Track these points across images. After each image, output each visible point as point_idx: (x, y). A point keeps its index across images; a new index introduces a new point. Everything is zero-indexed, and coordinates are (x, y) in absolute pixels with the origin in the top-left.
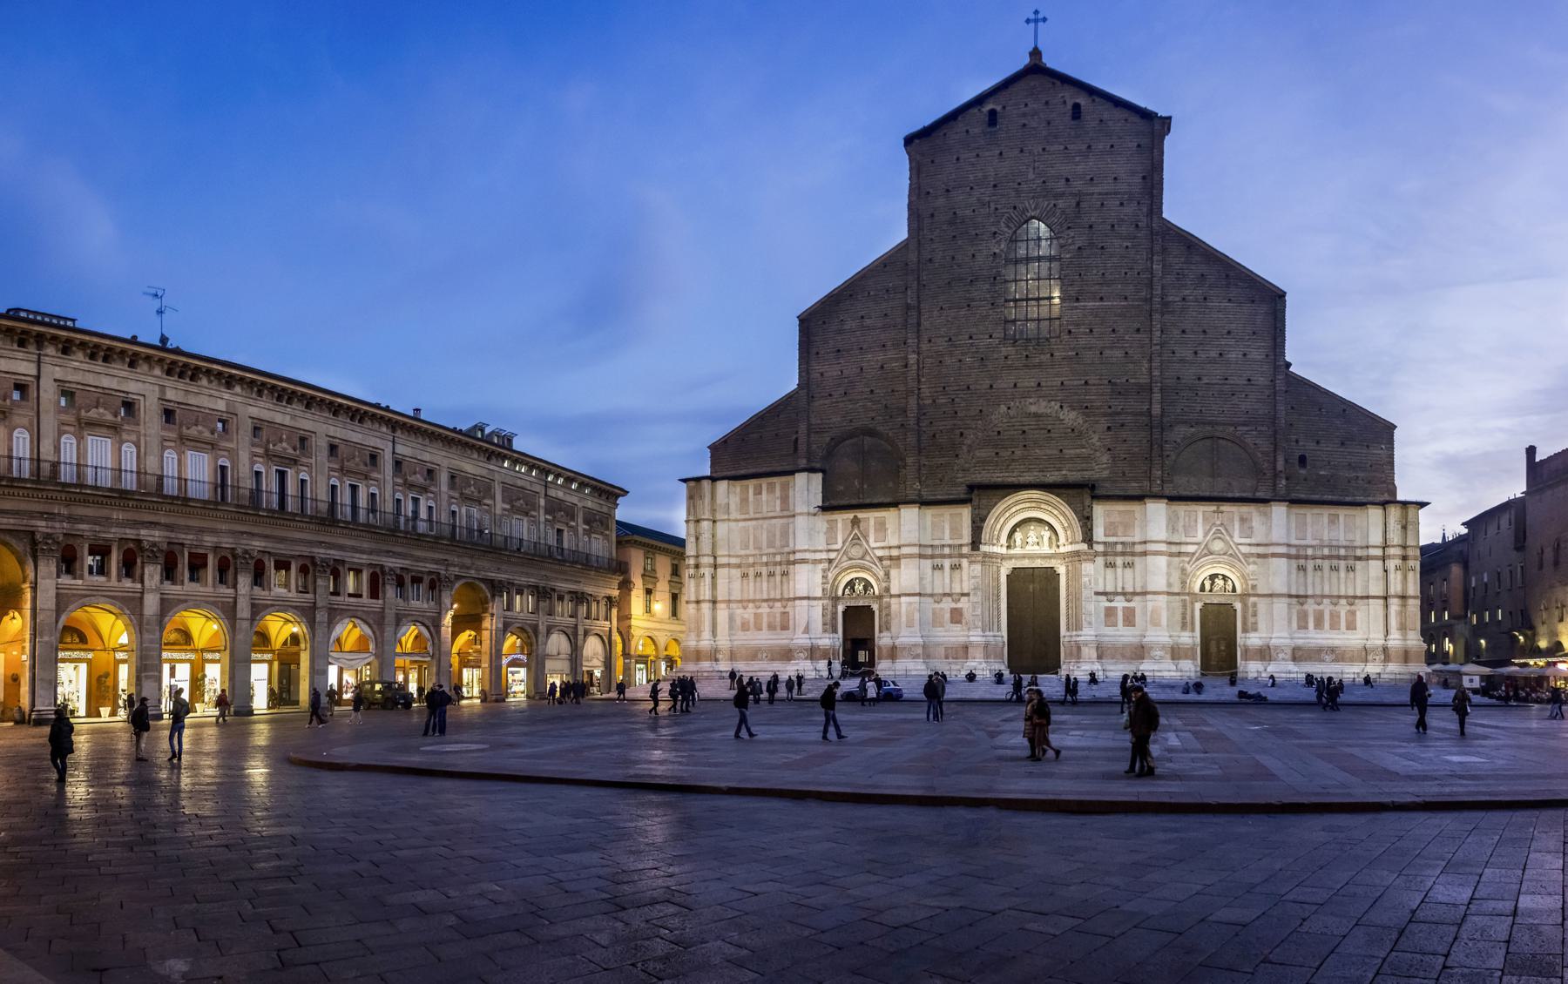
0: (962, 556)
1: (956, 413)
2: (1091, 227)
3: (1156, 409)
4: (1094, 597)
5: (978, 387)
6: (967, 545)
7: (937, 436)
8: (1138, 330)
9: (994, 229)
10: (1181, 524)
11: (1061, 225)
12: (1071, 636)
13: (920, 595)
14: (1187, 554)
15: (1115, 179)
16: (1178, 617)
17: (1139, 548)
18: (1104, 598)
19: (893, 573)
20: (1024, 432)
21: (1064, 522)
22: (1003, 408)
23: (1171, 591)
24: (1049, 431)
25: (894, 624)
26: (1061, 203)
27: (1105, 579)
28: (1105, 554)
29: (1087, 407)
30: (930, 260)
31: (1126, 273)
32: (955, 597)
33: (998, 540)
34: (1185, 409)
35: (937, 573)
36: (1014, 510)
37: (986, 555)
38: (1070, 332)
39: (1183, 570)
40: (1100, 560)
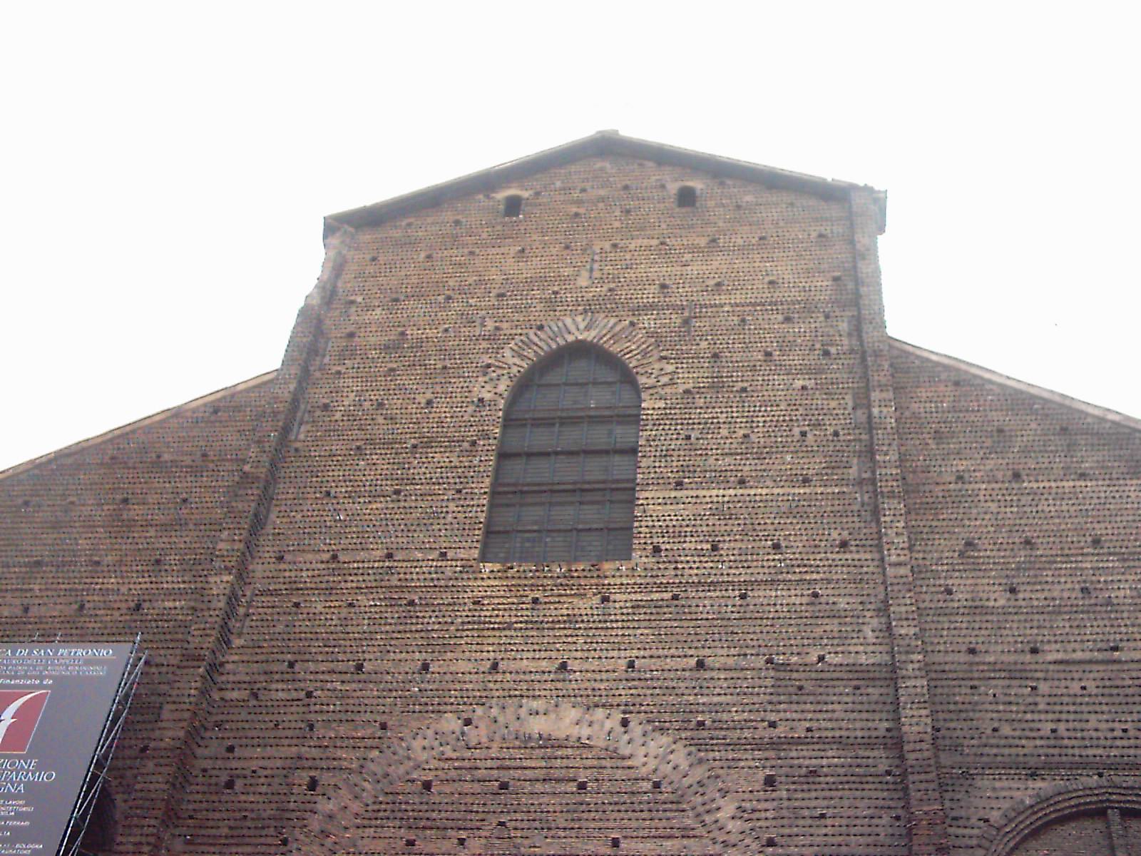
1: (311, 727)
2: (715, 356)
3: (915, 722)
5: (387, 665)
7: (239, 784)
8: (844, 544)
9: (486, 360)
11: (645, 354)
15: (771, 282)
20: (504, 786)
22: (451, 723)
24: (582, 786)
26: (647, 321)
29: (701, 724)
30: (326, 407)
31: (804, 434)
34: (1006, 730)
38: (657, 550)
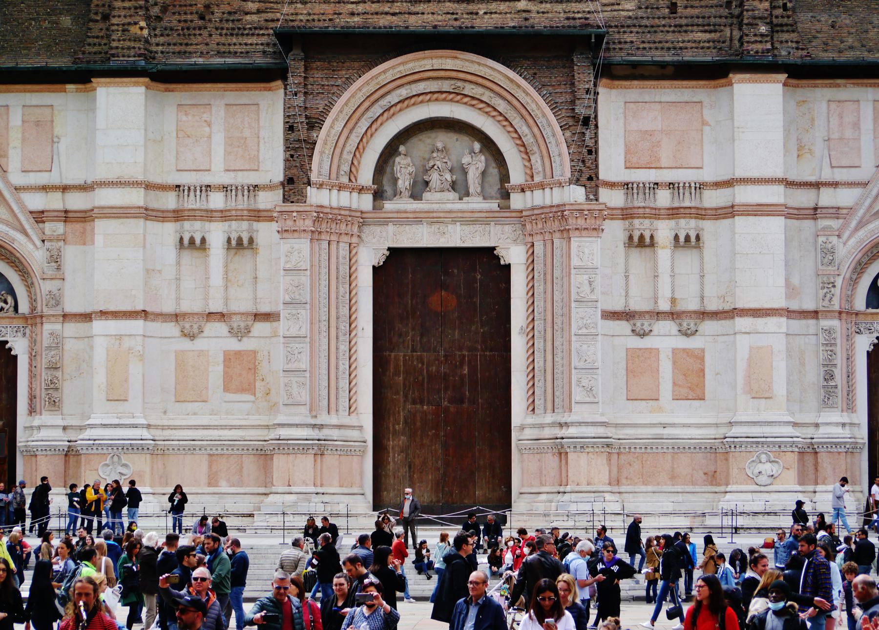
0: (257, 215)
4: (601, 323)
6: (269, 187)
10: (820, 133)
12: (542, 426)
13: (144, 314)
14: (836, 212)
16: (813, 374)
17: (713, 199)
18: (624, 327)
19: (71, 254)
21: (523, 129)
23: (794, 306)
25: (69, 391)
27: (627, 277)
28: (627, 214)
32: (236, 322)
33: (352, 174)
35: (188, 257)
36: (393, 98)
37: (322, 215)
39: (828, 253)
40: (615, 230)
